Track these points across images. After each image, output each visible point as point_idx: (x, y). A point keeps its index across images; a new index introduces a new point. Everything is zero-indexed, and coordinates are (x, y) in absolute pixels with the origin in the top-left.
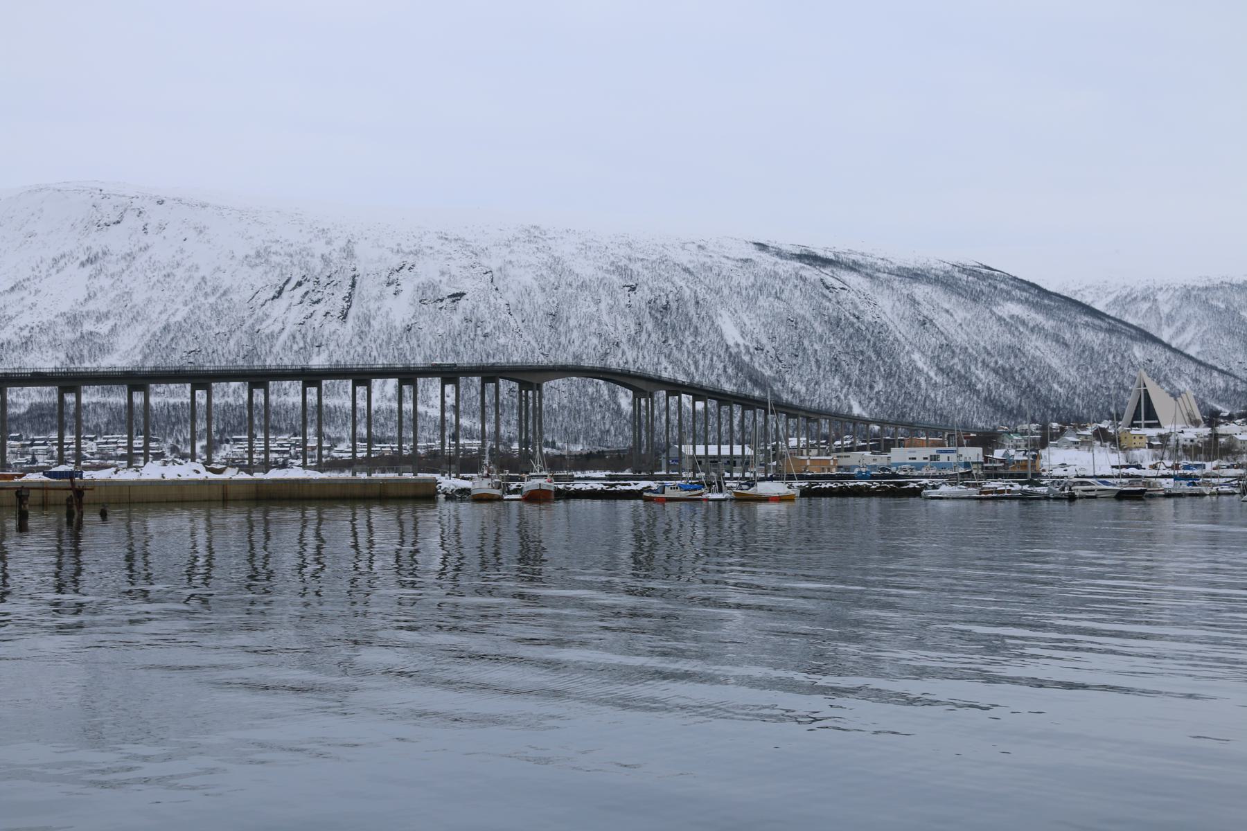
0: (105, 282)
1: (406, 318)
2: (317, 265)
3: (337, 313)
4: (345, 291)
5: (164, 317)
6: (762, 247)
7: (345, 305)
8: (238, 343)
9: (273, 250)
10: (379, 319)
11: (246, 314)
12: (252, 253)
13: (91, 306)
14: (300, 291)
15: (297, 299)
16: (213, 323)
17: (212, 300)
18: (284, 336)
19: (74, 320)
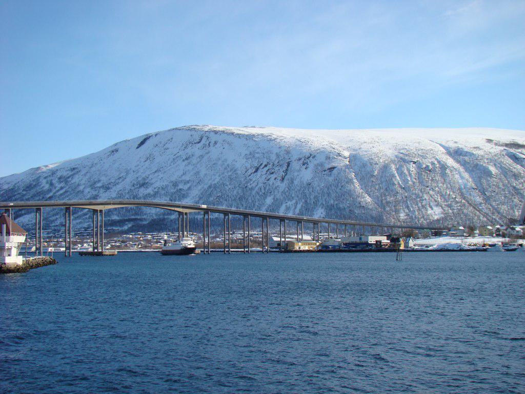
0: (190, 167)
1: (309, 179)
2: (273, 157)
3: (280, 178)
4: (285, 168)
5: (210, 182)
6: (489, 141)
7: (284, 174)
8: (237, 193)
9: (257, 151)
10: (298, 180)
11: (242, 180)
12: (248, 153)
13: (184, 178)
14: (266, 169)
15: (265, 172)
16: (228, 183)
17: (230, 174)
18: (257, 188)
19: (175, 184)
